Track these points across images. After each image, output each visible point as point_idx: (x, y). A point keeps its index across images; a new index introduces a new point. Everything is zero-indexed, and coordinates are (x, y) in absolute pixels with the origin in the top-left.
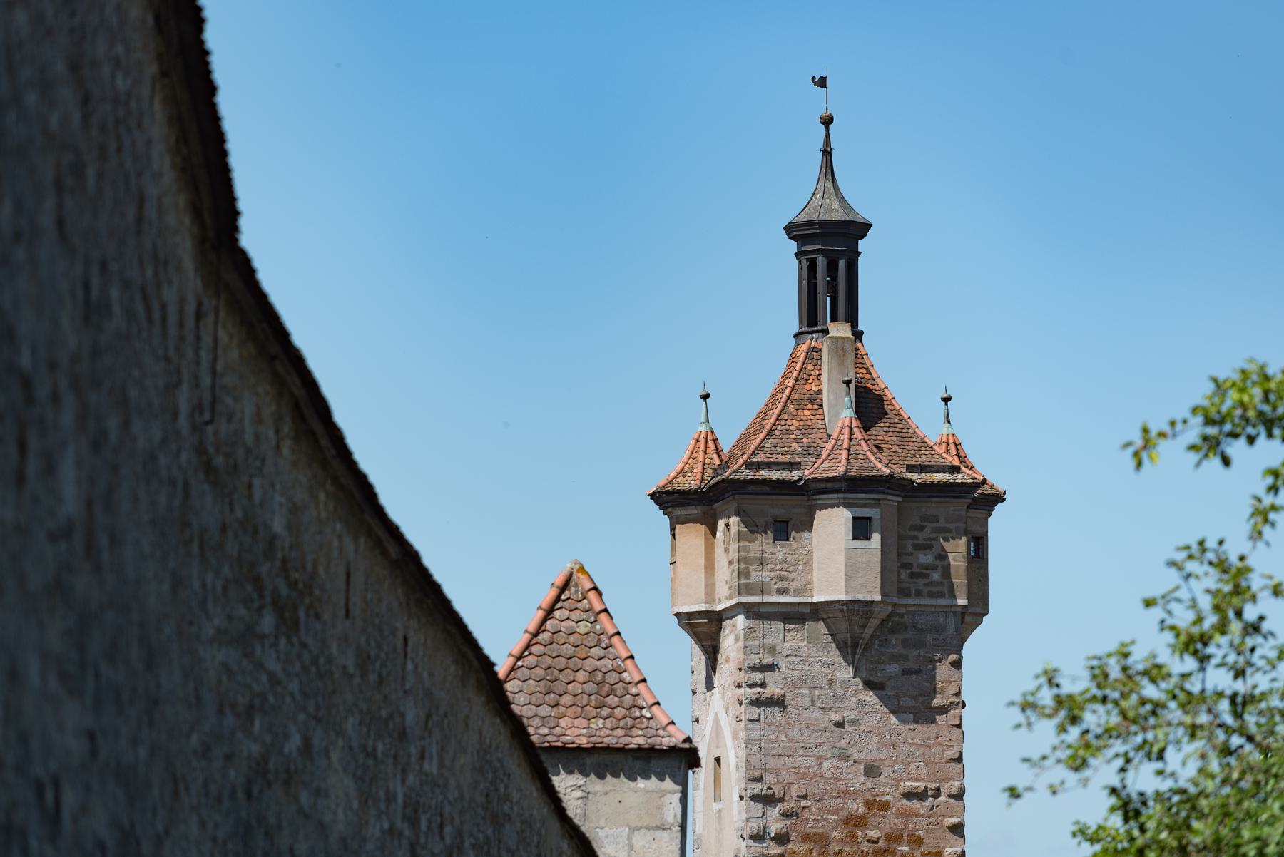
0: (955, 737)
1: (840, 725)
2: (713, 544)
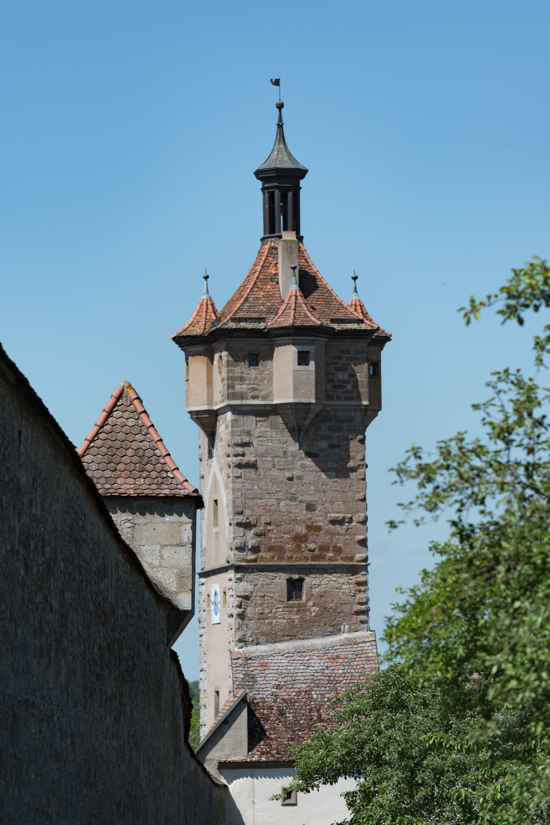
0: (361, 486)
1: (291, 479)
2: (212, 369)
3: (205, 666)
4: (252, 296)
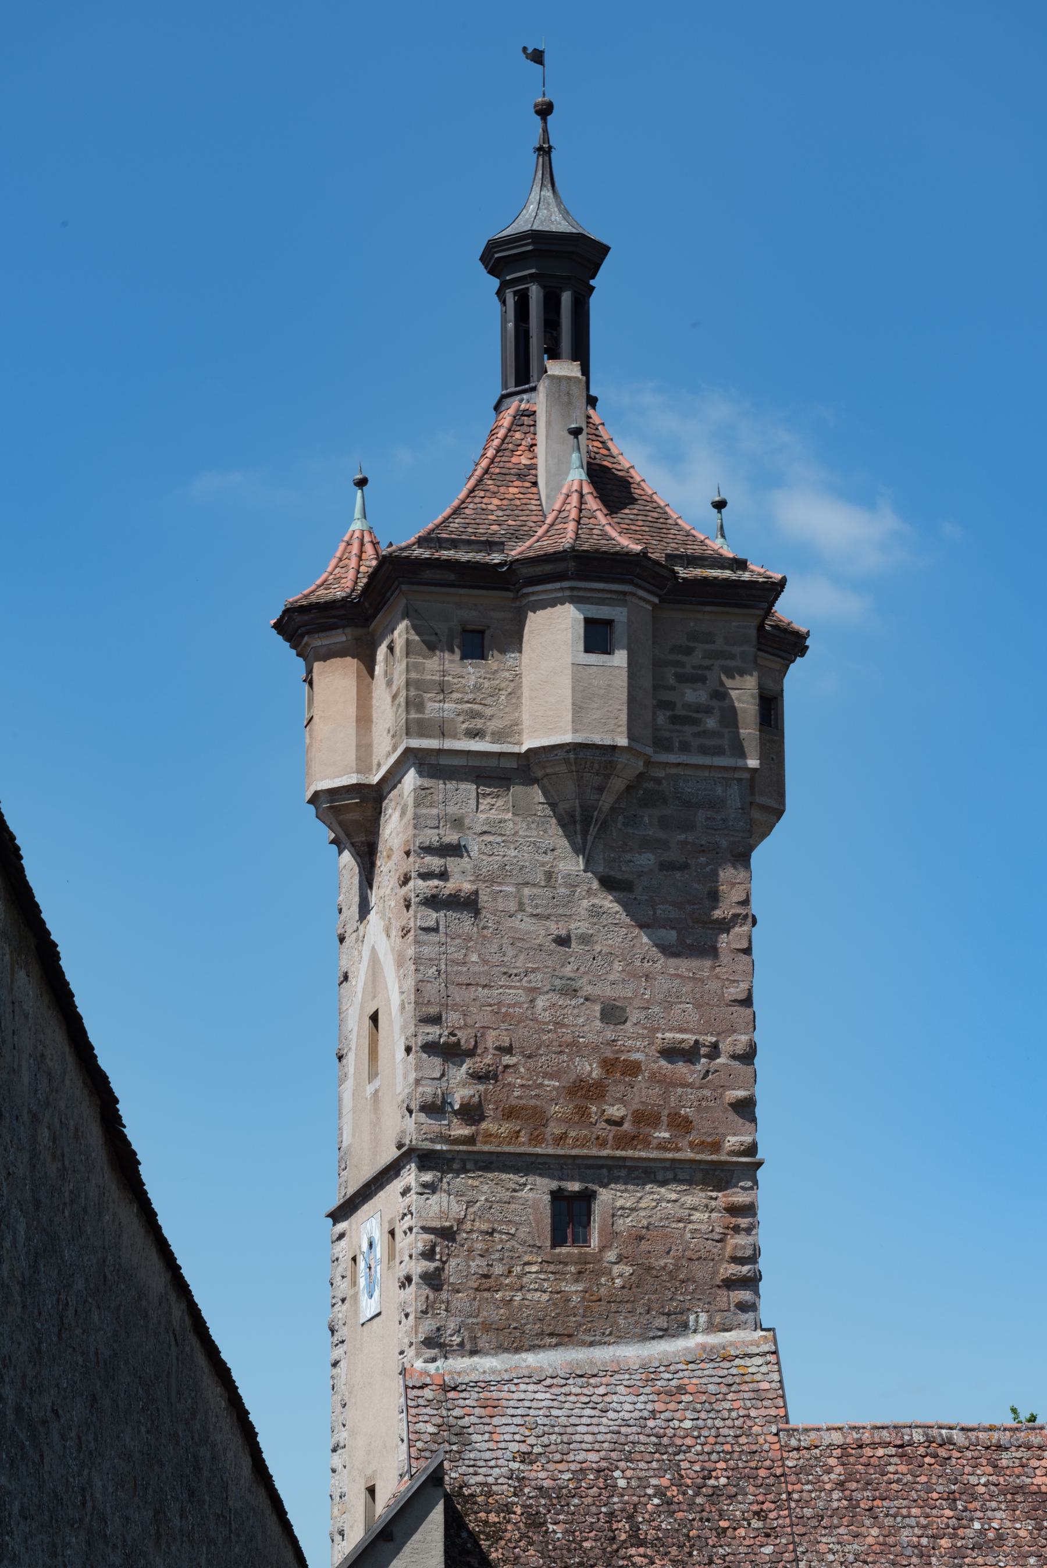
0: (740, 968)
1: (563, 941)
2: (369, 687)
3: (343, 1436)
4: (471, 506)
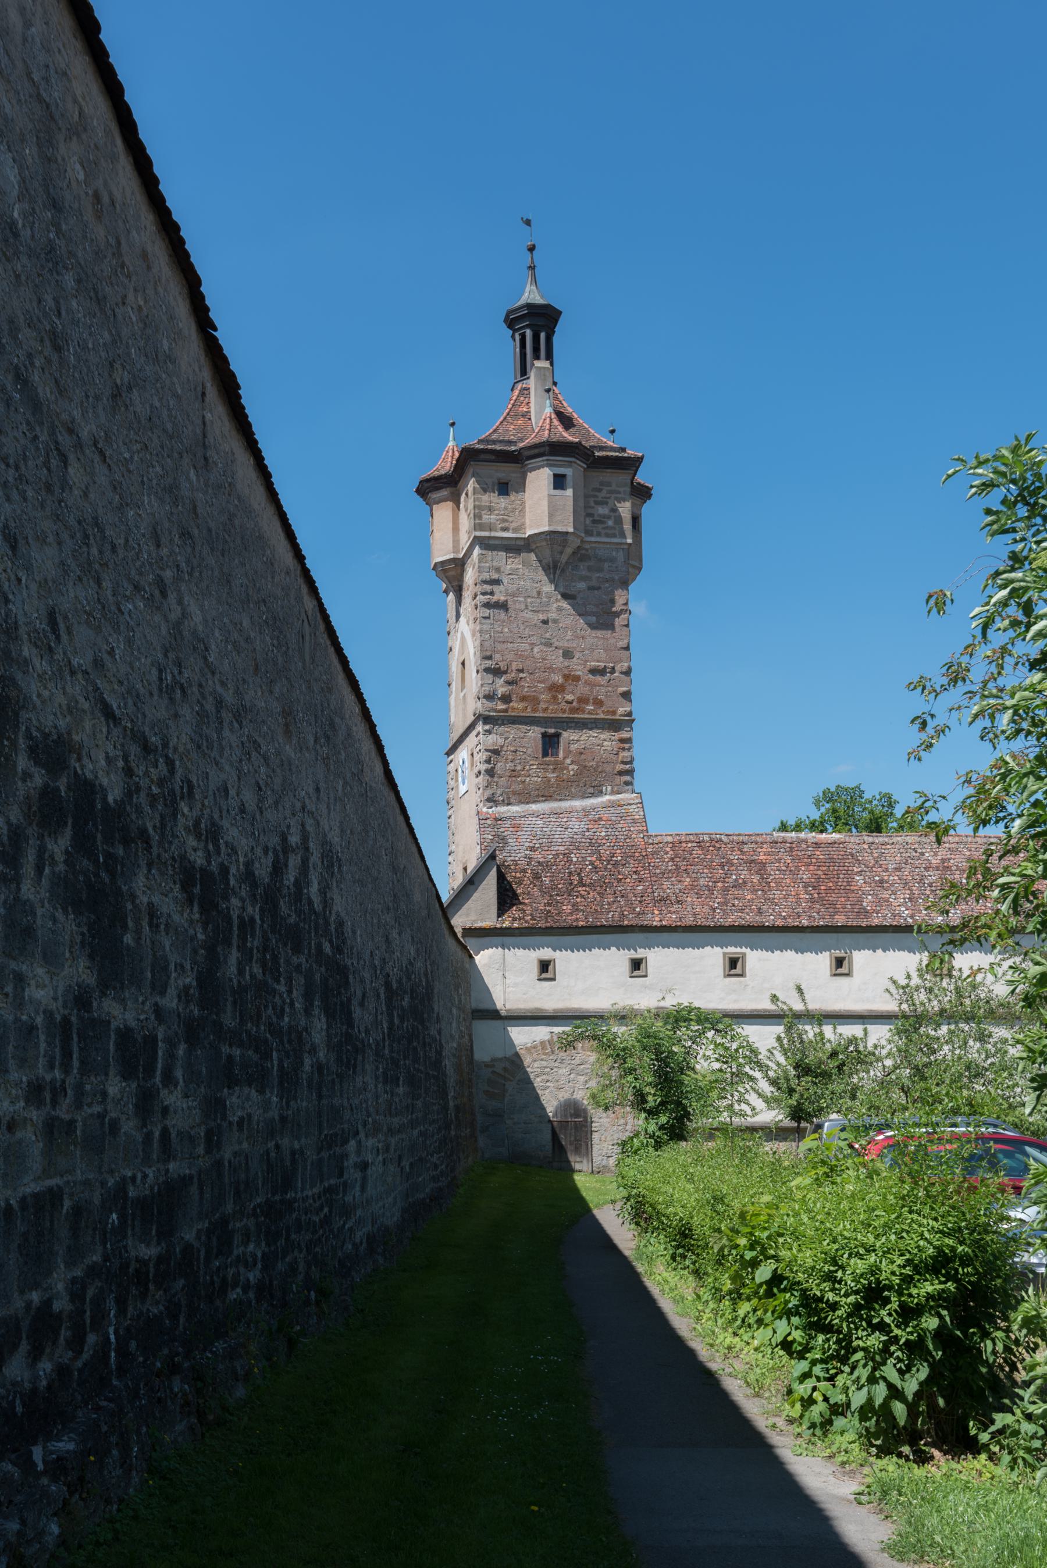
1: (545, 622)
3: (453, 847)
